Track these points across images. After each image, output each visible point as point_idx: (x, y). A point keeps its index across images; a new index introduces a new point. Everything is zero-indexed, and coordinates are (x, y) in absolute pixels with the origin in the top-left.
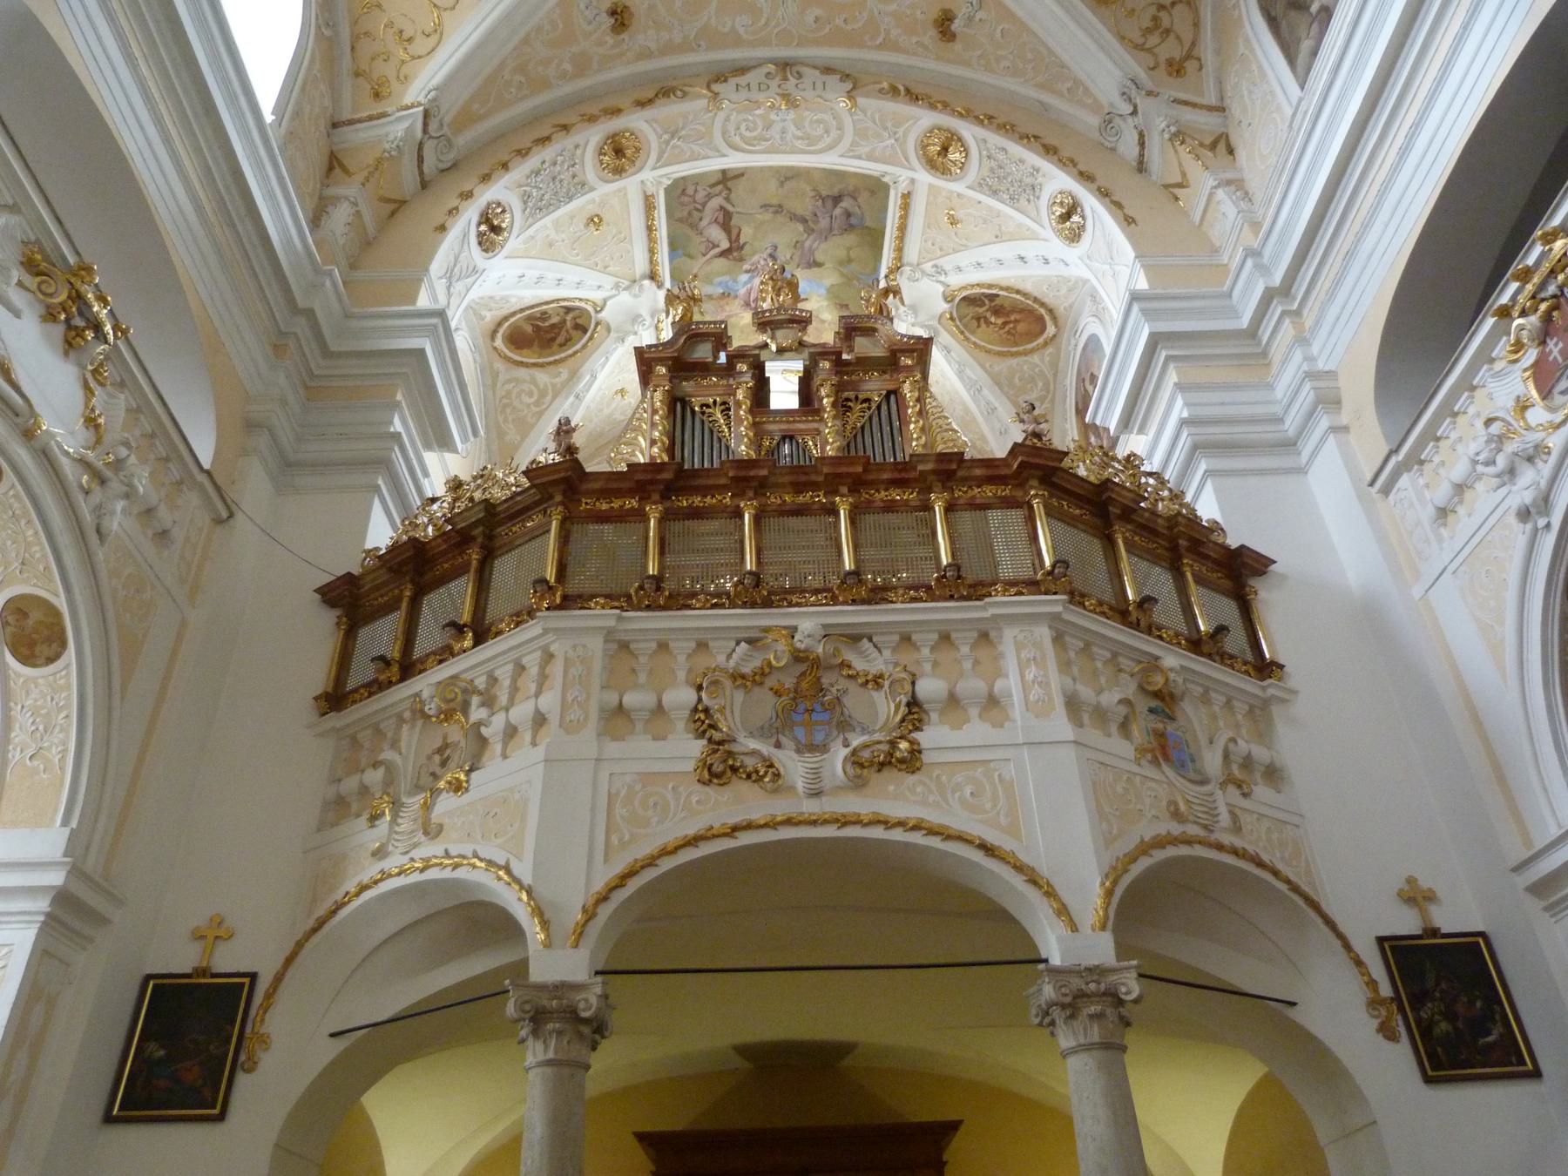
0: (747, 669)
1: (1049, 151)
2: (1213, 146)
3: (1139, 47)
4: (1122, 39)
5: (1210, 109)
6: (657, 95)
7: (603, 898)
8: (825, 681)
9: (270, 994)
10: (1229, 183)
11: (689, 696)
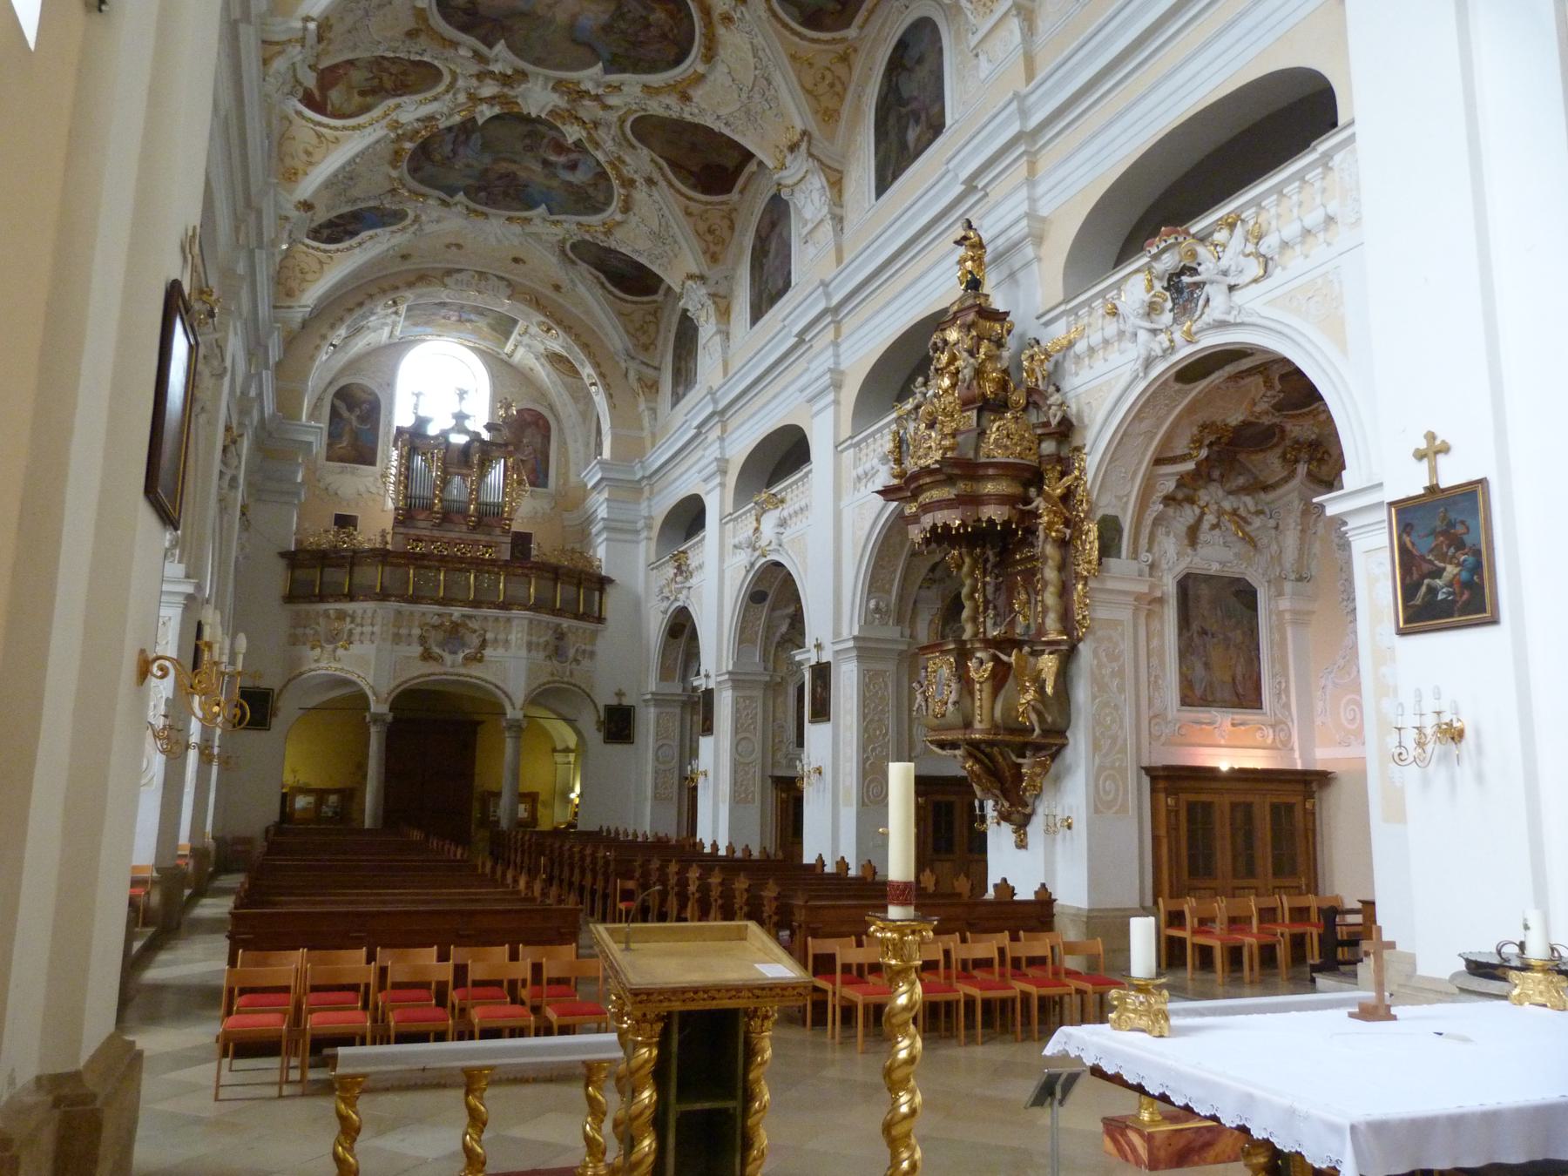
2: (651, 387)
4: (627, 332)
5: (655, 368)
7: (392, 691)
9: (279, 695)
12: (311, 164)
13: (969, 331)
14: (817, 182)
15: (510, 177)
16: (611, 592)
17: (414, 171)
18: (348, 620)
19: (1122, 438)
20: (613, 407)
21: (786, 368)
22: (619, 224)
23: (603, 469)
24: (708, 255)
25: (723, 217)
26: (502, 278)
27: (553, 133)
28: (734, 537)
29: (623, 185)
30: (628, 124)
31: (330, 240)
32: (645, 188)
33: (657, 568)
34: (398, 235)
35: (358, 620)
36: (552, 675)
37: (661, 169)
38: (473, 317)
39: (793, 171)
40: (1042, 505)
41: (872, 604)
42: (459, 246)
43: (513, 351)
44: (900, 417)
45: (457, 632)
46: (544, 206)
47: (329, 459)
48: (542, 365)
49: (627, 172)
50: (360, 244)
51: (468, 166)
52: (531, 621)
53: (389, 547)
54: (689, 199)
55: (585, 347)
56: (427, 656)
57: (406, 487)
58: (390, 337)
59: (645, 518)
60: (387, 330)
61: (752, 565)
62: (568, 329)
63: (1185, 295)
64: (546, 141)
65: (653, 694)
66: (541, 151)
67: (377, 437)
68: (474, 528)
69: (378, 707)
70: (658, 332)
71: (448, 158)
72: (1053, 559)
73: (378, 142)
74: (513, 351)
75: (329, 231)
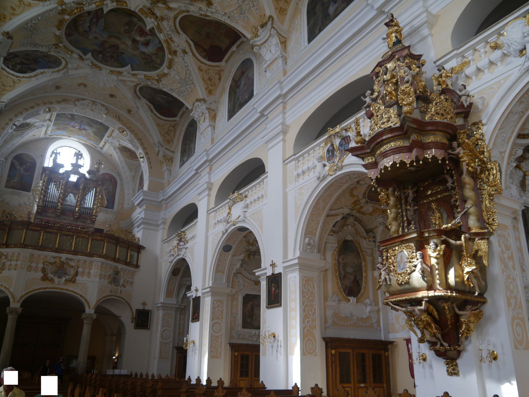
0: (52, 262)
1: (142, 144)
2: (169, 160)
3: (163, 136)
4: (160, 133)
6: (62, 100)
7: (23, 296)
8: (64, 266)
10: (169, 170)
11: (42, 266)
12: (14, 14)
13: (405, 60)
14: (275, 40)
15: (115, 47)
16: (143, 254)
17: (68, 35)
18: (3, 257)
19: (508, 114)
20: (150, 167)
21: (250, 133)
22: (165, 75)
23: (144, 195)
24: (208, 90)
25: (216, 73)
26: (103, 105)
27: (140, 24)
28: (215, 219)
29: (170, 53)
30: (178, 20)
31: (20, 71)
32: (182, 54)
33: (167, 242)
34: (55, 74)
35: (9, 258)
36: (111, 292)
37: (190, 46)
38: (86, 127)
39: (261, 37)
40: (462, 152)
41: (307, 240)
42: (85, 86)
43: (104, 146)
44: (330, 137)
45: (63, 267)
46: (129, 65)
47: (6, 187)
48: (117, 153)
49: (173, 46)
50: (36, 75)
51: (96, 38)
52: (103, 263)
53: (32, 220)
54: (202, 62)
55: (139, 139)
56: (45, 278)
57: (44, 196)
58: (46, 133)
59: (163, 218)
60: (44, 129)
61: (226, 231)
62: (132, 131)
64: (136, 27)
65: (161, 303)
66: (133, 33)
67: (32, 179)
68: (77, 219)
69: (15, 305)
70: (175, 135)
71: (86, 32)
72: (469, 184)
73: (51, 10)
74: (104, 146)
75: (20, 66)
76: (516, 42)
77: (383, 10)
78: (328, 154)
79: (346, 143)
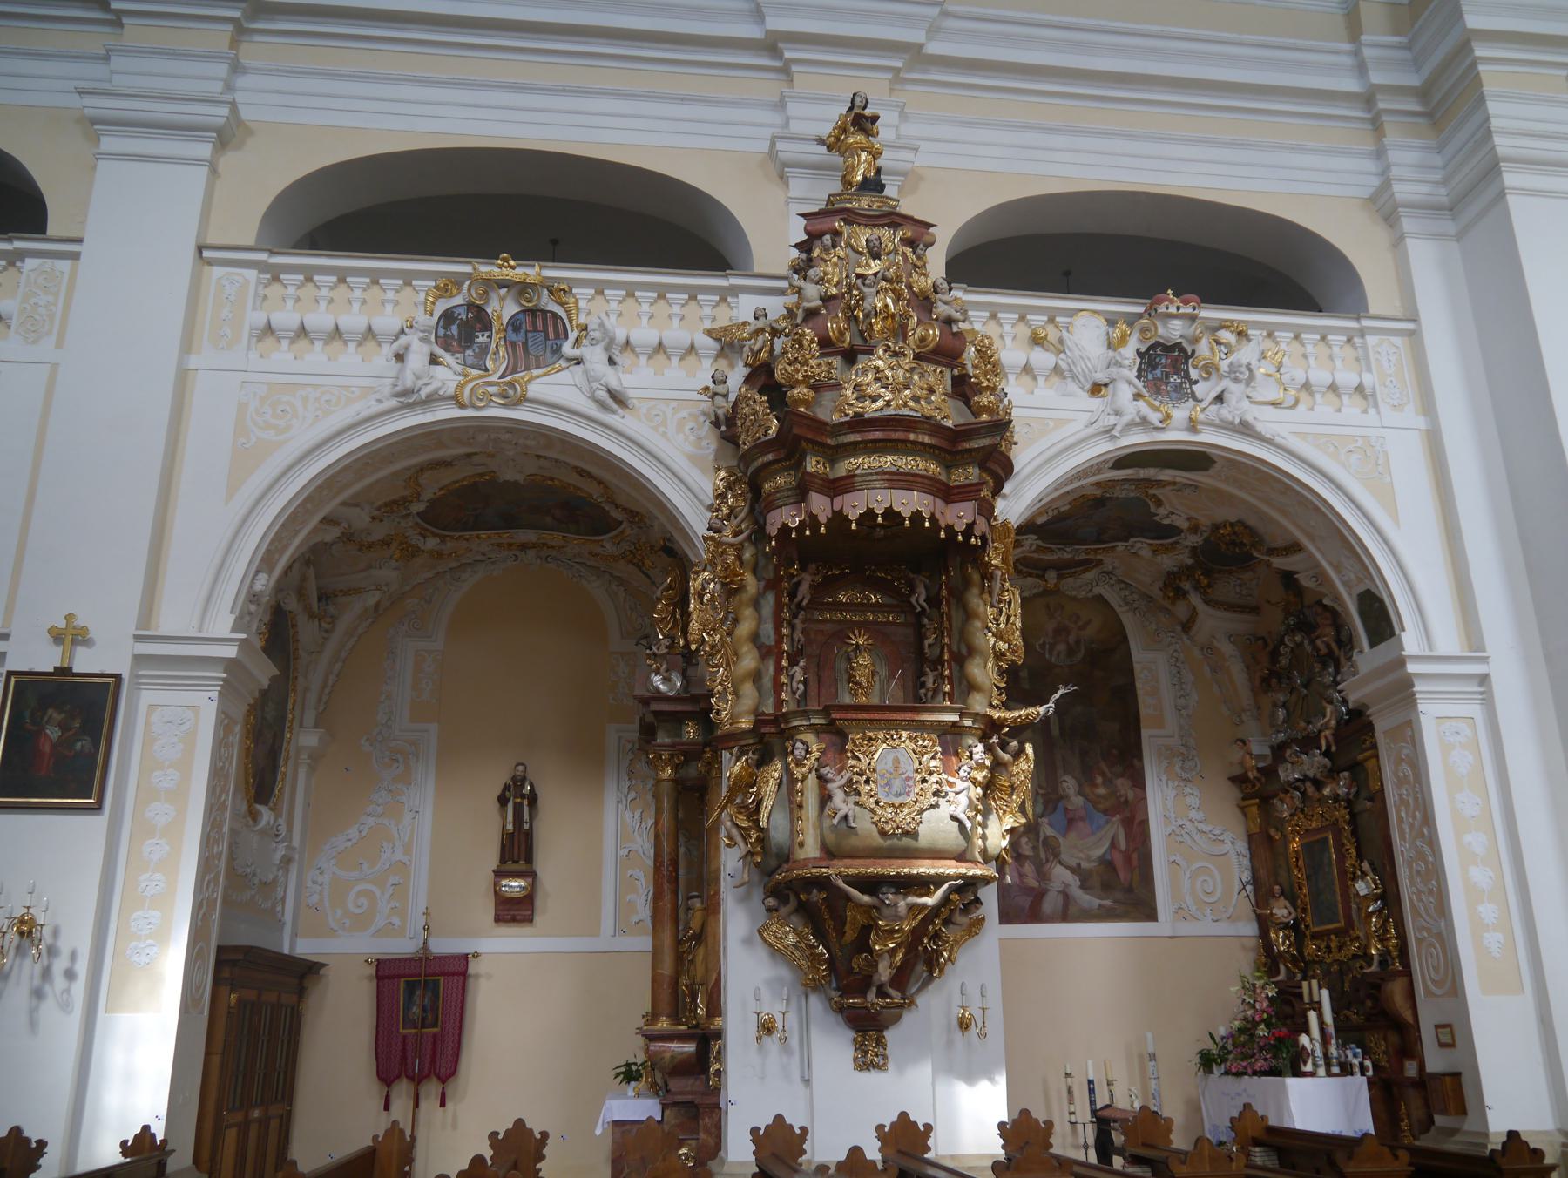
63: (1158, 372)
76: (1089, 359)
77: (780, 45)
78: (445, 328)
79: (535, 330)
